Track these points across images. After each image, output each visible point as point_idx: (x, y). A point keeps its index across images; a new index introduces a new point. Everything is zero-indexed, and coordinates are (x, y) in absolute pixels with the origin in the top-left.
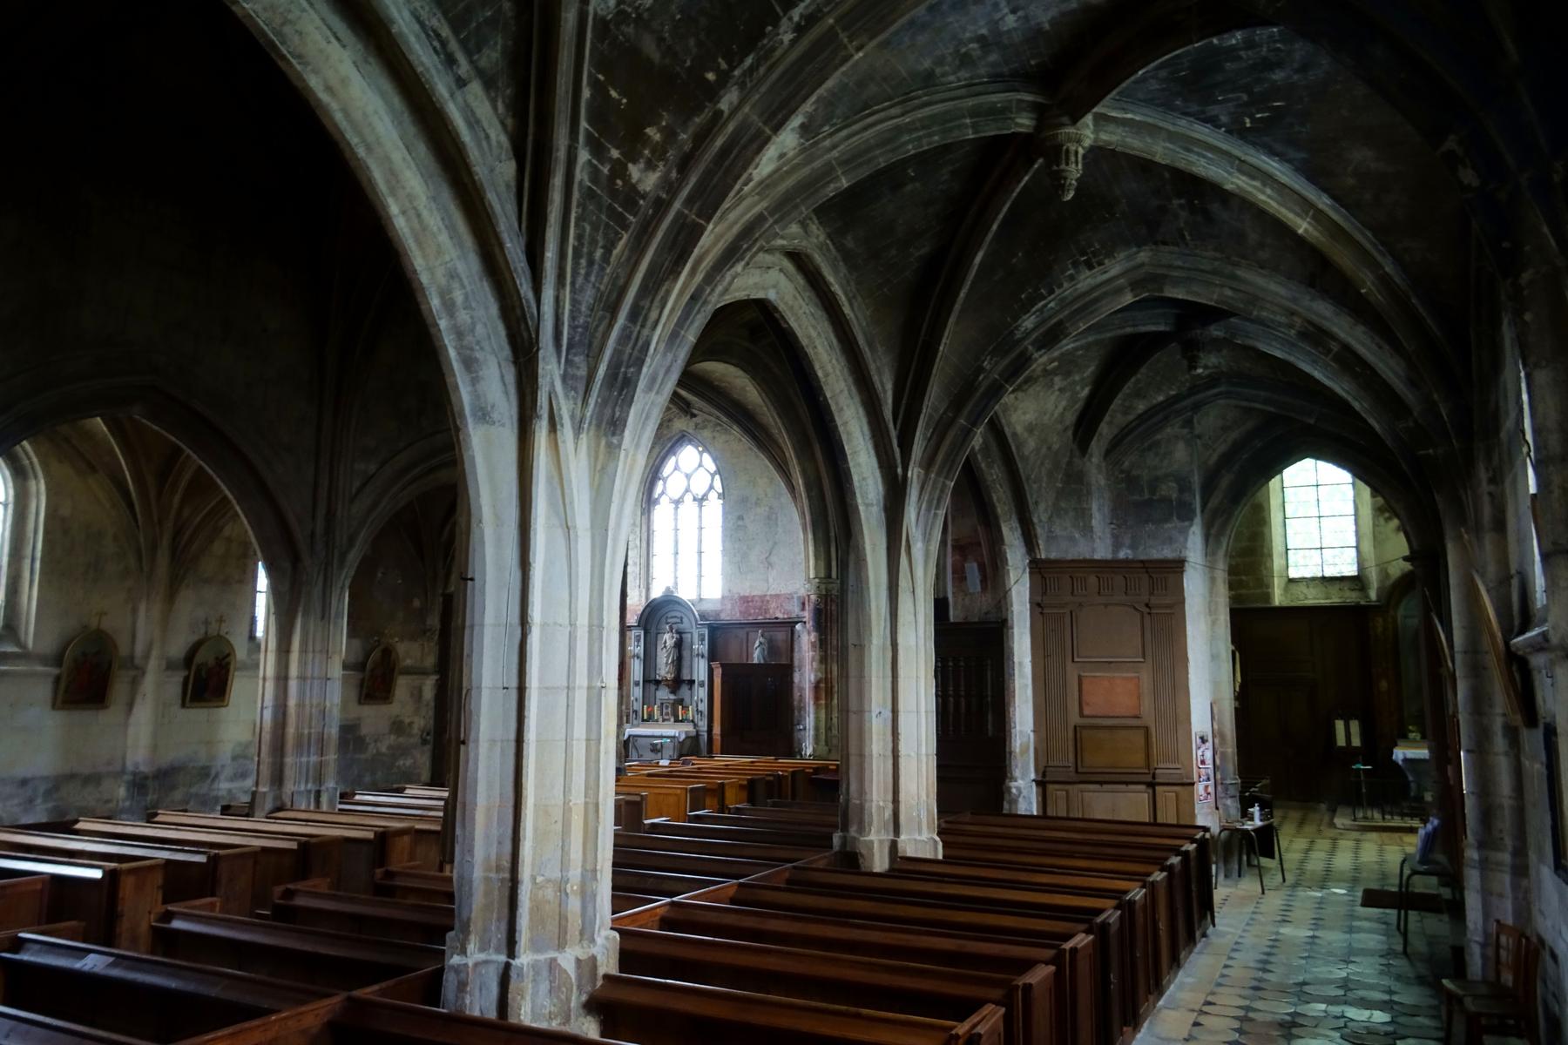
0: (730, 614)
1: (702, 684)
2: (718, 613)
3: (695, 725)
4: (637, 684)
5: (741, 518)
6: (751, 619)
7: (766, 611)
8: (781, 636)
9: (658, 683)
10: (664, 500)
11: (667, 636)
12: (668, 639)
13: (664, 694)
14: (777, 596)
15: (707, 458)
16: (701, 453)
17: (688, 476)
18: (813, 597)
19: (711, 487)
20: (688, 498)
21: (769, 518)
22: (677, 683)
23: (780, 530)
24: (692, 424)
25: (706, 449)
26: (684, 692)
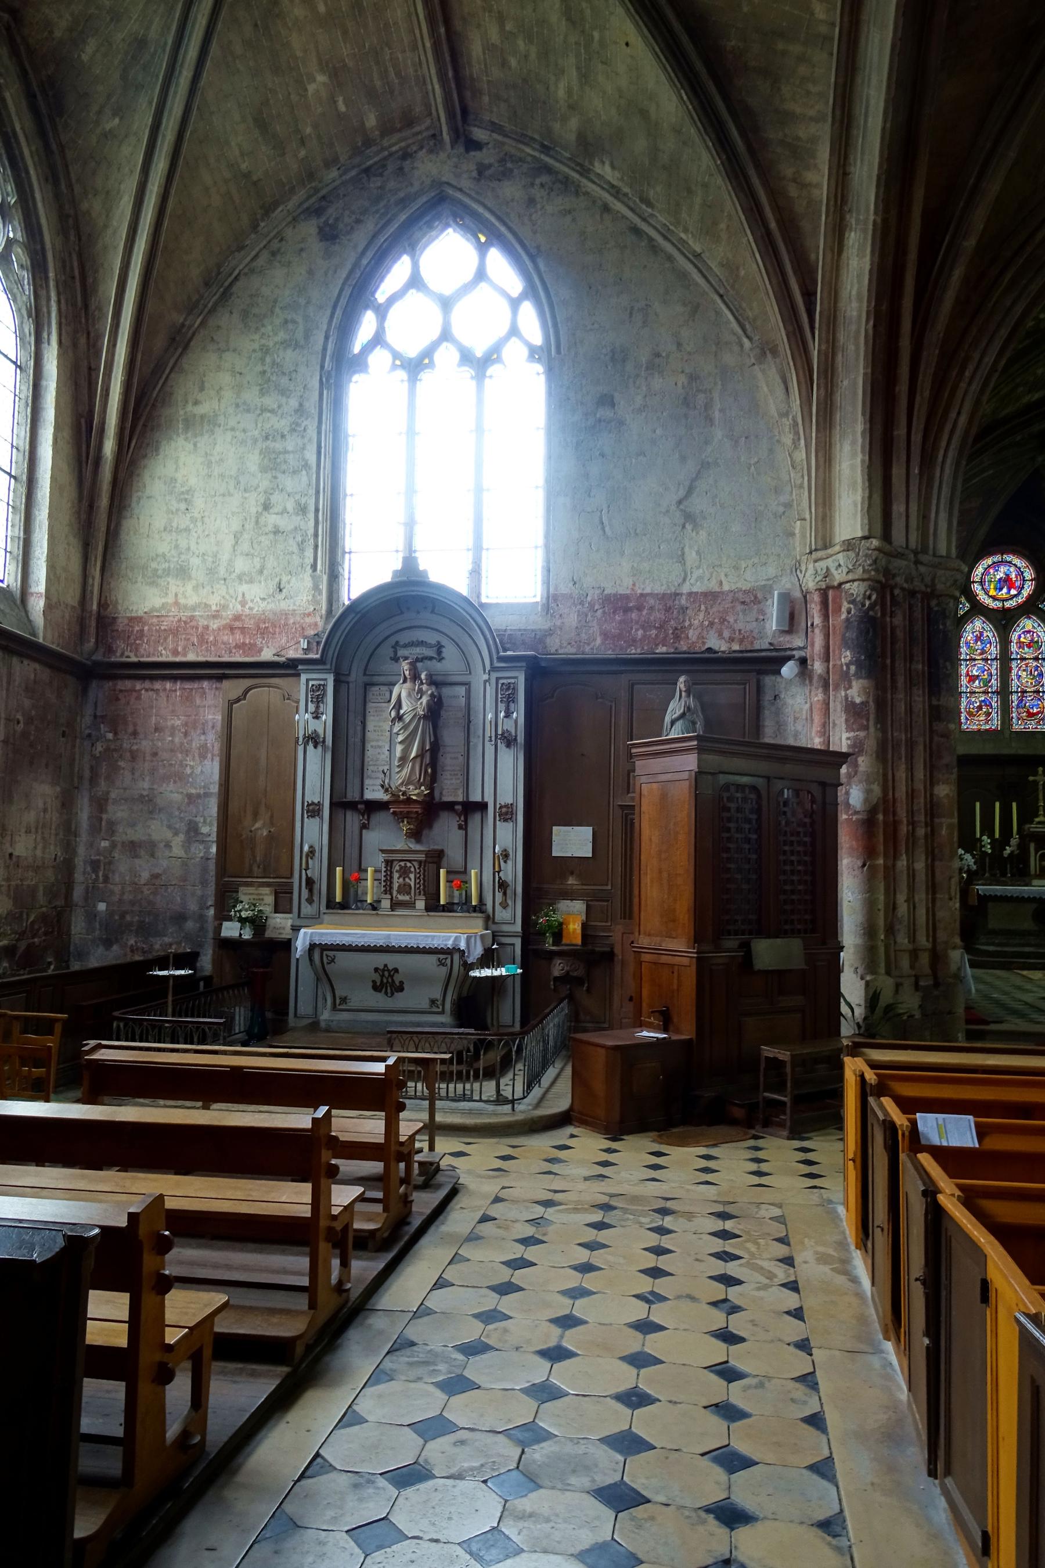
0: (580, 637)
1: (506, 814)
2: (539, 639)
3: (489, 920)
4: (314, 810)
5: (607, 400)
6: (634, 652)
7: (679, 633)
8: (727, 693)
9: (374, 807)
10: (379, 359)
11: (402, 690)
12: (408, 698)
13: (384, 838)
14: (711, 597)
15: (498, 261)
16: (482, 250)
17: (446, 304)
18: (856, 589)
19: (514, 331)
20: (446, 356)
21: (686, 402)
22: (424, 813)
23: (719, 434)
24: (469, 166)
25: (496, 238)
26: (446, 833)
